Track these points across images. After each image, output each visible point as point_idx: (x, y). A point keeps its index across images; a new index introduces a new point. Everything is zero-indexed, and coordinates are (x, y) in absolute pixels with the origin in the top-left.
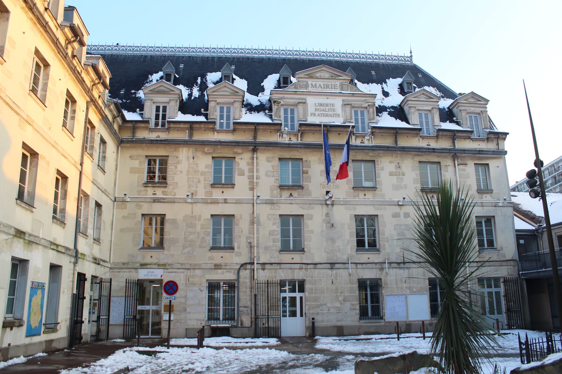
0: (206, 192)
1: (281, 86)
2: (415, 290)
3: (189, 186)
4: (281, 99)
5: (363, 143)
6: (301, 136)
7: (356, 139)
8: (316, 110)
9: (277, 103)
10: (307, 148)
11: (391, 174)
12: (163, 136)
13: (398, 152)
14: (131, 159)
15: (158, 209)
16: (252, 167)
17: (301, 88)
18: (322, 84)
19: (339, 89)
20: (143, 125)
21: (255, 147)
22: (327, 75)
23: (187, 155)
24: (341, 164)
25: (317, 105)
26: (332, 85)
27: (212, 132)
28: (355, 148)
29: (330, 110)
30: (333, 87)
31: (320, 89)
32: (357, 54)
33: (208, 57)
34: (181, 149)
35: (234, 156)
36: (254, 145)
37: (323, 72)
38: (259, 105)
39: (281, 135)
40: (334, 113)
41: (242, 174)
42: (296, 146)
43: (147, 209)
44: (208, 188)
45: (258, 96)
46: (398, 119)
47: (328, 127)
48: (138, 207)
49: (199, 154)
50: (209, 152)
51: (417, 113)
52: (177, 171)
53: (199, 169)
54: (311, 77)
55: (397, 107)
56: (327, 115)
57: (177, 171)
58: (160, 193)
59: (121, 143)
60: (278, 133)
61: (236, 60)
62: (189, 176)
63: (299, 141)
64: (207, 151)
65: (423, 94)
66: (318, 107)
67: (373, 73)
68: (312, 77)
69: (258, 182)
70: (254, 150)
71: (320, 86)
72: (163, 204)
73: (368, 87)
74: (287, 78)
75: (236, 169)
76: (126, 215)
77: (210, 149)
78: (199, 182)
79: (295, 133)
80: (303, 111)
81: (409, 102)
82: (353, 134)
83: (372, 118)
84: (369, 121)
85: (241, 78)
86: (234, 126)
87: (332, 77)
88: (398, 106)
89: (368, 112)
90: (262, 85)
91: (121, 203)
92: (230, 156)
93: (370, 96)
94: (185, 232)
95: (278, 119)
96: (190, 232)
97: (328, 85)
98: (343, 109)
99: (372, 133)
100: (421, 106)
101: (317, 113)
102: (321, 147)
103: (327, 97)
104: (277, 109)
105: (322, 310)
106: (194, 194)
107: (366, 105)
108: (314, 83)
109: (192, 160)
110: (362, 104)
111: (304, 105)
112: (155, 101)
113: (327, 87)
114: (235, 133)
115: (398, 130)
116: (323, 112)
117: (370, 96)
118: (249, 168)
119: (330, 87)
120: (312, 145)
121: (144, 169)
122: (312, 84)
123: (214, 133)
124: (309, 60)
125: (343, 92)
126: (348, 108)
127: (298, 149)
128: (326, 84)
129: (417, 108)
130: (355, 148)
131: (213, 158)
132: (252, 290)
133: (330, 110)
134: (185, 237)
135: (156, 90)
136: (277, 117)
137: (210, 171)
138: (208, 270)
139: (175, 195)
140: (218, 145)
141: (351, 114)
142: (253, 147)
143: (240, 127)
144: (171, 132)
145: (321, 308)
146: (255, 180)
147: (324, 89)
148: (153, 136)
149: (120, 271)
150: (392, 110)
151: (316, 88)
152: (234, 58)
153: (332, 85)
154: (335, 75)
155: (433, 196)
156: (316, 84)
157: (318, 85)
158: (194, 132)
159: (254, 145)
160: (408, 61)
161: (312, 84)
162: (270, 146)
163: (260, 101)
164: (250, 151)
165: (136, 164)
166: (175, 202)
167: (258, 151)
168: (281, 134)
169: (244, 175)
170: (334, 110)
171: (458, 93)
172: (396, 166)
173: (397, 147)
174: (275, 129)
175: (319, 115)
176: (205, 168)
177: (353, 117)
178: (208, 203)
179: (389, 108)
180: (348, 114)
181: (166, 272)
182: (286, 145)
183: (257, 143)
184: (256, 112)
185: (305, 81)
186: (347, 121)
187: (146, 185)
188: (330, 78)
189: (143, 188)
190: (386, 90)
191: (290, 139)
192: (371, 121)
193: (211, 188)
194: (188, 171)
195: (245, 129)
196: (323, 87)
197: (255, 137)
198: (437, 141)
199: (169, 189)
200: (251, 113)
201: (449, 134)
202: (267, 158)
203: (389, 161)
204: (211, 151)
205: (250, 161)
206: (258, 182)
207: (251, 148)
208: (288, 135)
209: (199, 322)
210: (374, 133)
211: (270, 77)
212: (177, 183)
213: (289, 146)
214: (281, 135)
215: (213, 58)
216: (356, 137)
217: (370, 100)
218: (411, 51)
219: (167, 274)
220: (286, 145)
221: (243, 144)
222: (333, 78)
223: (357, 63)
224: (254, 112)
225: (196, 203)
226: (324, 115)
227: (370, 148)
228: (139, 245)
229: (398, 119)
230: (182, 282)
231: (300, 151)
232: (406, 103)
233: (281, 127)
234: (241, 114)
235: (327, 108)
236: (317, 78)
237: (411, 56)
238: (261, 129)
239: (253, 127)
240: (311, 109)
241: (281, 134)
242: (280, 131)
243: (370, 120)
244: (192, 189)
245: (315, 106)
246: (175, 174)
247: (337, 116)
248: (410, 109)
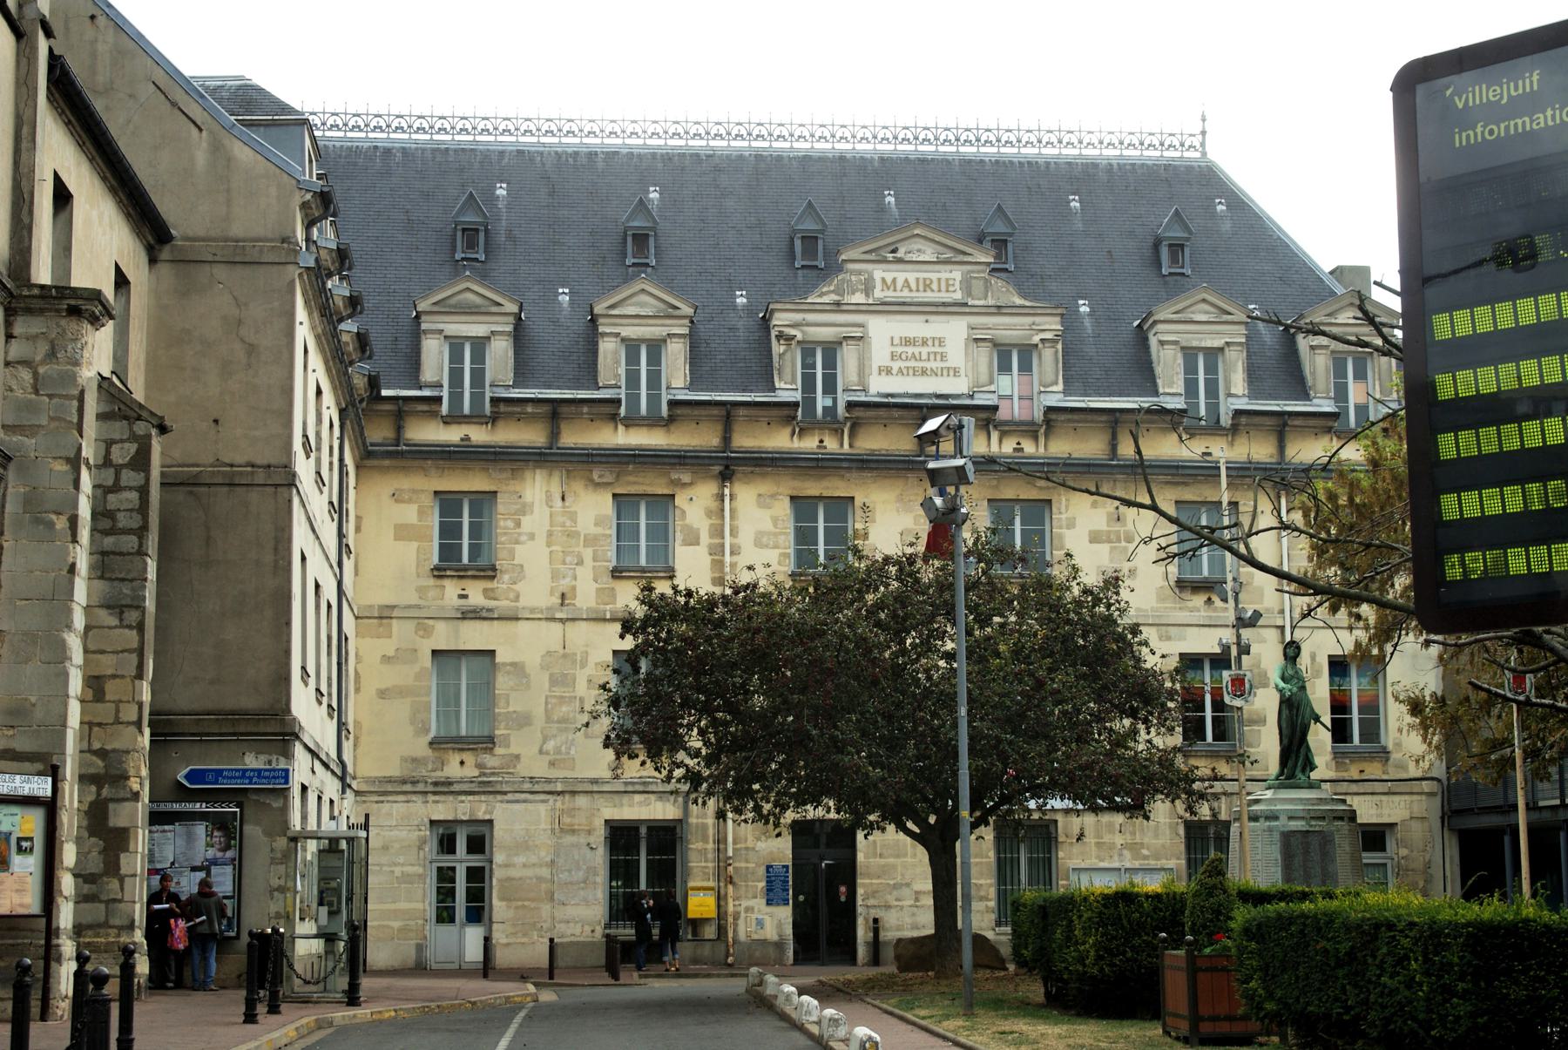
0: (598, 590)
2: (1145, 852)
3: (555, 575)
6: (852, 435)
7: (1000, 442)
11: (1095, 538)
12: (479, 435)
14: (396, 501)
15: (474, 636)
16: (719, 522)
20: (425, 407)
21: (727, 467)
23: (544, 490)
25: (896, 341)
26: (939, 280)
27: (612, 425)
29: (932, 357)
30: (943, 287)
33: (576, 153)
34: (528, 474)
41: (692, 540)
43: (443, 636)
44: (605, 579)
48: (421, 633)
49: (578, 486)
50: (605, 480)
52: (520, 534)
53: (579, 529)
56: (924, 372)
57: (520, 534)
58: (476, 594)
59: (368, 457)
62: (554, 548)
64: (600, 477)
65: (1204, 300)
66: (900, 349)
67: (1072, 204)
69: (736, 564)
70: (726, 476)
72: (486, 623)
75: (678, 529)
76: (391, 653)
77: (608, 473)
78: (580, 563)
81: (1160, 327)
91: (375, 621)
94: (547, 697)
96: (562, 697)
99: (1048, 422)
101: (896, 366)
103: (923, 318)
105: (897, 900)
106: (568, 596)
109: (559, 503)
112: (449, 334)
113: (927, 286)
114: (672, 428)
115: (1118, 414)
116: (912, 364)
118: (711, 525)
119: (935, 286)
121: (432, 527)
122: (883, 280)
123: (616, 428)
124: (882, 159)
127: (843, 472)
128: (925, 279)
131: (615, 495)
132: (722, 846)
133: (932, 357)
134: (546, 711)
135: (453, 301)
137: (608, 532)
138: (608, 795)
139: (517, 598)
140: (627, 463)
142: (721, 468)
144: (500, 424)
145: (895, 893)
146: (728, 558)
148: (451, 435)
149: (381, 798)
153: (939, 280)
155: (1209, 599)
156: (894, 280)
157: (900, 284)
158: (562, 426)
159: (725, 462)
161: (883, 280)
164: (713, 477)
165: (409, 513)
166: (517, 619)
169: (698, 544)
170: (943, 357)
171: (1327, 269)
172: (1109, 514)
176: (596, 524)
178: (605, 620)
181: (502, 802)
185: (866, 271)
187: (439, 572)
189: (432, 582)
191: (821, 441)
193: (610, 580)
194: (550, 534)
196: (913, 286)
197: (726, 439)
198: (1232, 444)
199: (501, 584)
201: (1268, 421)
202: (760, 495)
204: (609, 478)
205: (714, 505)
206: (736, 564)
207: (717, 469)
209: (588, 929)
212: (522, 566)
213: (820, 465)
215: (592, 155)
216: (1003, 435)
219: (504, 805)
225: (573, 620)
228: (428, 731)
230: (543, 826)
235: (925, 350)
237: (1203, 133)
240: (880, 353)
244: (562, 582)
246: (517, 542)
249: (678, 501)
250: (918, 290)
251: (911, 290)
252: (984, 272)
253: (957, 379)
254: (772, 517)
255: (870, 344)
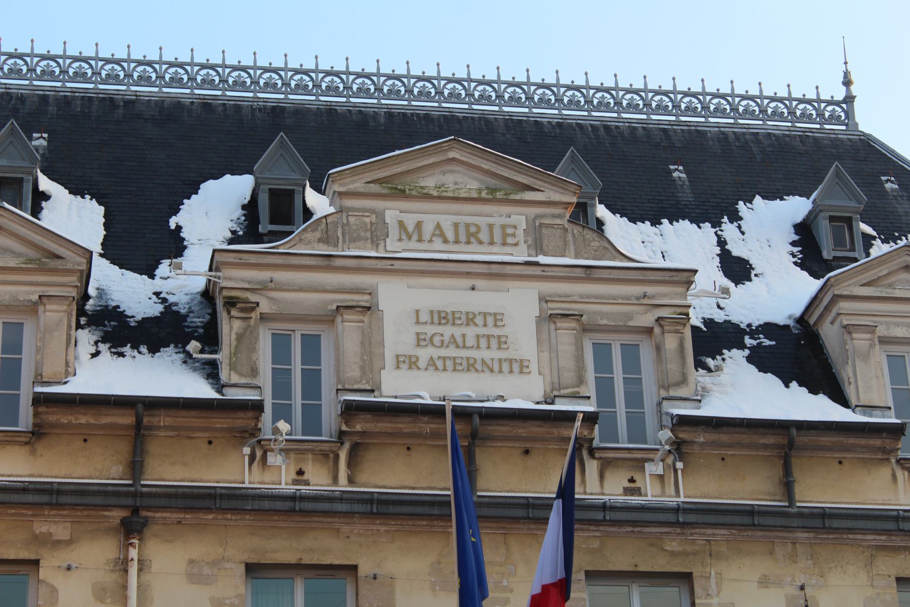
1: (261, 229)
4: (262, 288)
5: (637, 491)
6: (350, 464)
7: (602, 477)
8: (420, 340)
9: (242, 310)
10: (379, 515)
13: (801, 535)
17: (353, 240)
18: (447, 222)
19: (523, 247)
21: (135, 511)
22: (471, 184)
24: (537, 590)
25: (424, 317)
26: (491, 226)
28: (599, 516)
29: (483, 343)
30: (497, 237)
31: (438, 244)
32: (607, 90)
35: (33, 557)
36: (129, 501)
37: (451, 172)
38: (156, 317)
39: (260, 457)
40: (503, 355)
42: (326, 506)
45: (152, 276)
46: (794, 385)
47: (477, 419)
51: (880, 356)
54: (400, 194)
55: (786, 327)
56: (470, 366)
60: (244, 445)
61: (52, 109)
63: (343, 485)
66: (430, 330)
68: (404, 191)
71: (439, 231)
73: (658, 239)
74: (290, 194)
79: (325, 447)
80: (362, 343)
81: (844, 306)
82: (592, 452)
83: (674, 376)
84: (663, 394)
85: (73, 191)
86: (36, 414)
87: (492, 190)
88: (791, 323)
89: (658, 349)
90: (173, 226)
92: (12, 557)
93: (666, 276)
95: (243, 381)
97: (473, 229)
98: (545, 336)
99: (679, 448)
100: (897, 325)
101: (424, 354)
102: (445, 511)
103: (468, 282)
104: (240, 337)
107: (647, 319)
108: (410, 221)
110: (629, 316)
111: (366, 319)
113: (472, 236)
114: (40, 447)
115: (794, 431)
116: (452, 352)
117: (666, 276)
120: (402, 503)
122: (401, 224)
124: (390, 115)
125: (542, 259)
126: (565, 335)
127: (337, 522)
128: (467, 226)
129: (882, 331)
130: (599, 516)
133: (483, 343)
136: (241, 375)
141: (579, 358)
143: (65, 418)
147: (456, 248)
150: (767, 342)
151: (420, 240)
152: (44, 99)
153: (491, 226)
154: (505, 185)
156: (419, 225)
159: (129, 501)
160: (833, 118)
161: (401, 224)
162: (208, 510)
163: (164, 300)
167: (147, 532)
168: (259, 453)
170: (502, 343)
173: (794, 510)
174: (230, 430)
175: (432, 363)
177: (590, 375)
179: (753, 332)
180: (567, 362)
182: (279, 505)
183: (143, 495)
184: (143, 349)
185: (373, 211)
186: (563, 392)
188: (484, 195)
190: (737, 249)
191: (300, 473)
192: (673, 393)
195: (88, 426)
196: (450, 235)
197: (136, 467)
200: (122, 355)
202: (191, 562)
203: (757, 579)
205: (110, 579)
207: (117, 515)
208: (292, 455)
210: (685, 449)
211: (209, 187)
214: (260, 457)
216: (605, 466)
217: (665, 295)
218: (846, 74)
220: (279, 505)
221: (79, 500)
222: (499, 195)
223: (607, 128)
224: (135, 347)
226: (455, 364)
227: (671, 517)
229: (794, 385)
231: (346, 529)
232: (827, 308)
233: (257, 419)
234: (71, 358)
235: (471, 332)
236: (428, 197)
237: (849, 99)
238: (166, 428)
239: (126, 419)
241: (259, 453)
242: (253, 435)
243: (667, 388)
245: (418, 322)
247: (516, 367)
248: (847, 337)
249: (43, 573)
250: (457, 242)
251: (446, 241)
252: (559, 216)
253: (524, 378)
254: (212, 599)
255: (381, 319)
